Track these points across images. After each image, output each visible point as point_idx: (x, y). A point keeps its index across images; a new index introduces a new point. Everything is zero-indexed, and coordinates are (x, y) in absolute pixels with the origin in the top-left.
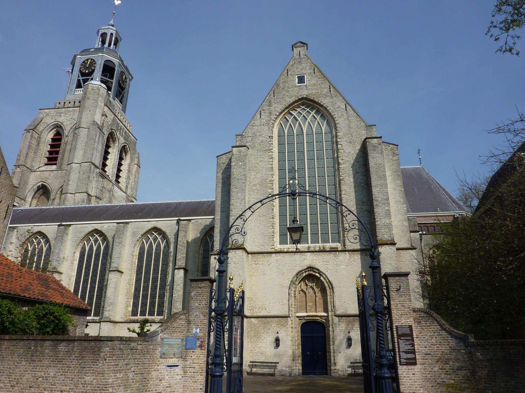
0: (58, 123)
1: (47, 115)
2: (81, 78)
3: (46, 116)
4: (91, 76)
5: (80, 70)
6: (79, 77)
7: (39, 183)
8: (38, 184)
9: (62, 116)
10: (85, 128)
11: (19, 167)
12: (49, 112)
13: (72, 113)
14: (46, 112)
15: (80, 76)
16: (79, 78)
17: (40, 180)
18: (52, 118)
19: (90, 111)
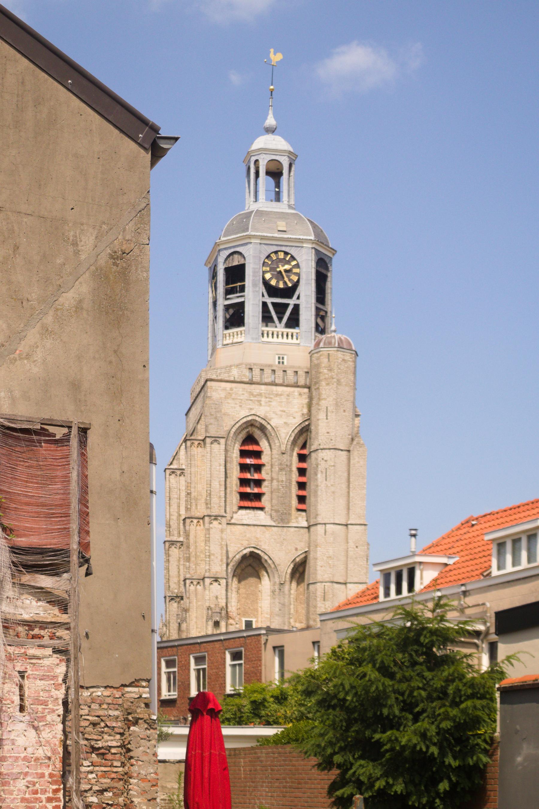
0: (257, 419)
1: (229, 395)
2: (269, 301)
3: (226, 398)
4: (290, 297)
5: (264, 278)
6: (263, 296)
7: (245, 549)
8: (245, 552)
9: (263, 403)
10: (342, 450)
11: (216, 519)
12: (231, 389)
13: (284, 399)
14: (225, 389)
15: (266, 294)
16: (265, 300)
17: (245, 543)
18: (241, 406)
19: (344, 411)
